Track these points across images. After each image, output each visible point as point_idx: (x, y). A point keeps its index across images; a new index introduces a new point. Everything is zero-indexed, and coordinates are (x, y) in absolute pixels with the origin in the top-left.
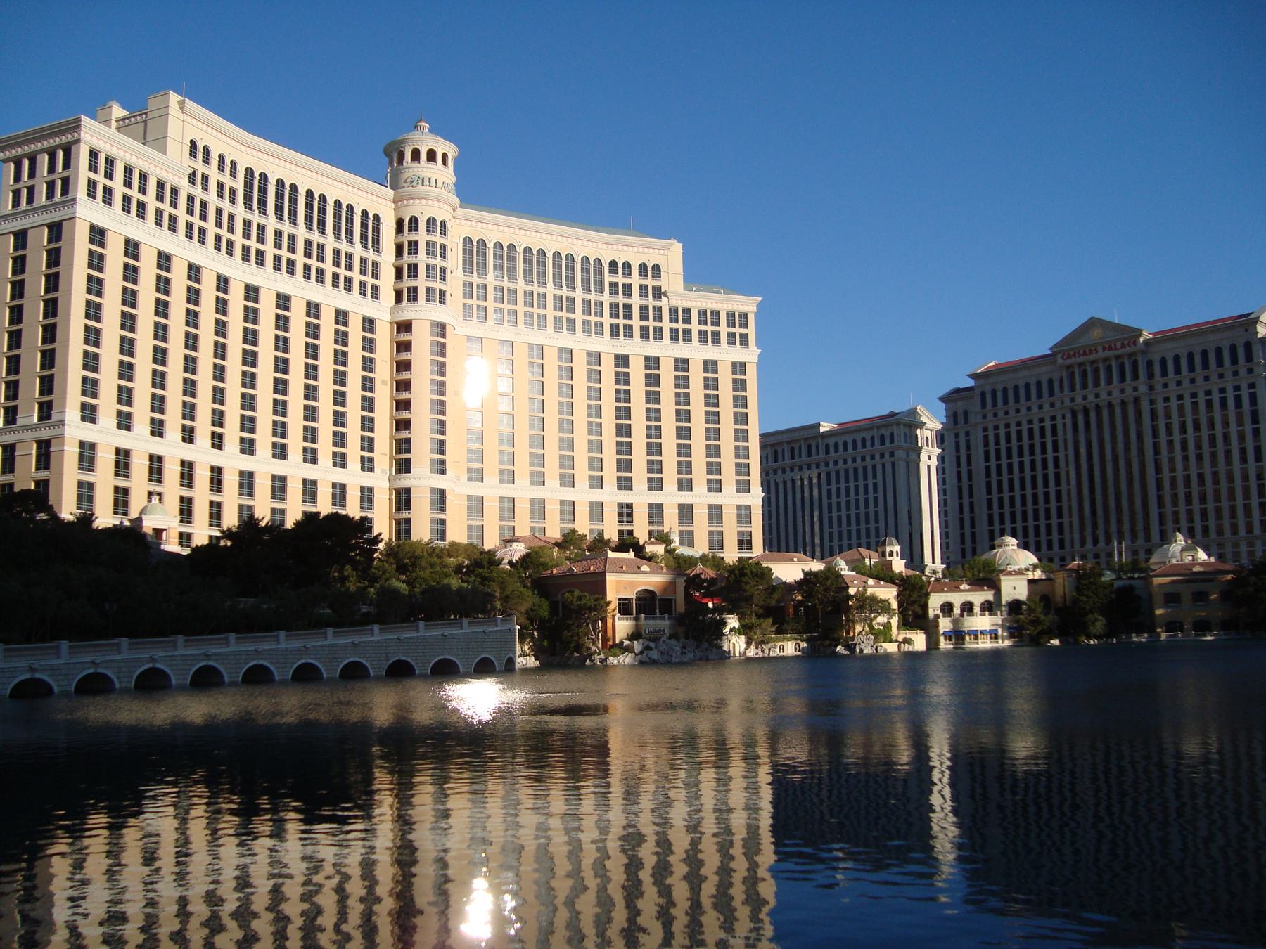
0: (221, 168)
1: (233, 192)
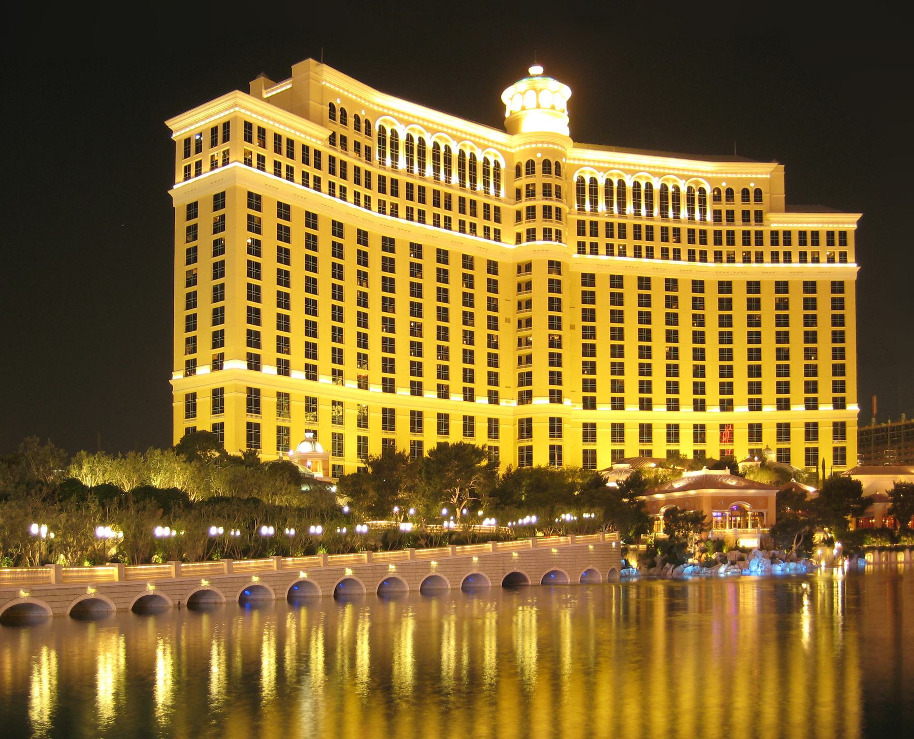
0: (357, 128)
1: (368, 150)
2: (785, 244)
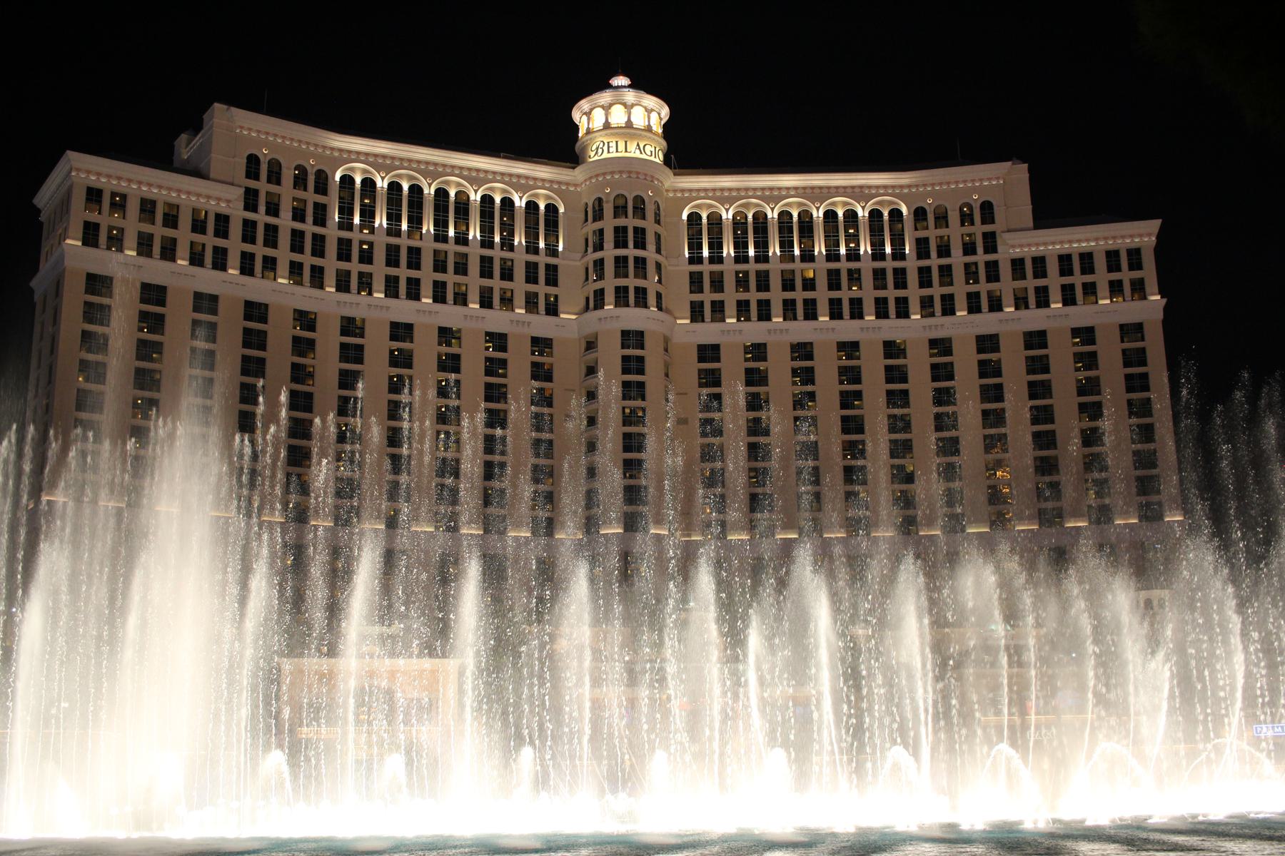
2: (1036, 276)
